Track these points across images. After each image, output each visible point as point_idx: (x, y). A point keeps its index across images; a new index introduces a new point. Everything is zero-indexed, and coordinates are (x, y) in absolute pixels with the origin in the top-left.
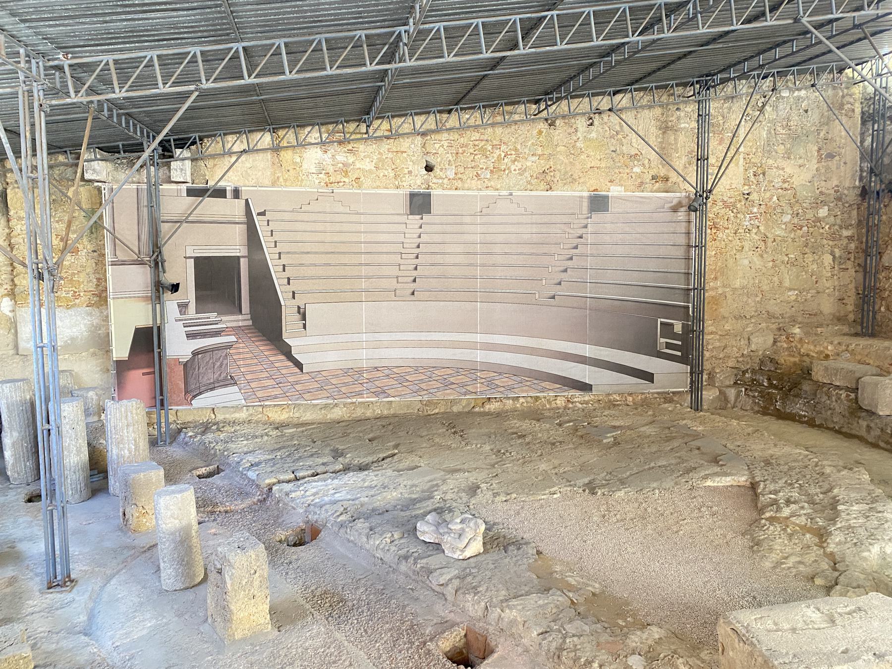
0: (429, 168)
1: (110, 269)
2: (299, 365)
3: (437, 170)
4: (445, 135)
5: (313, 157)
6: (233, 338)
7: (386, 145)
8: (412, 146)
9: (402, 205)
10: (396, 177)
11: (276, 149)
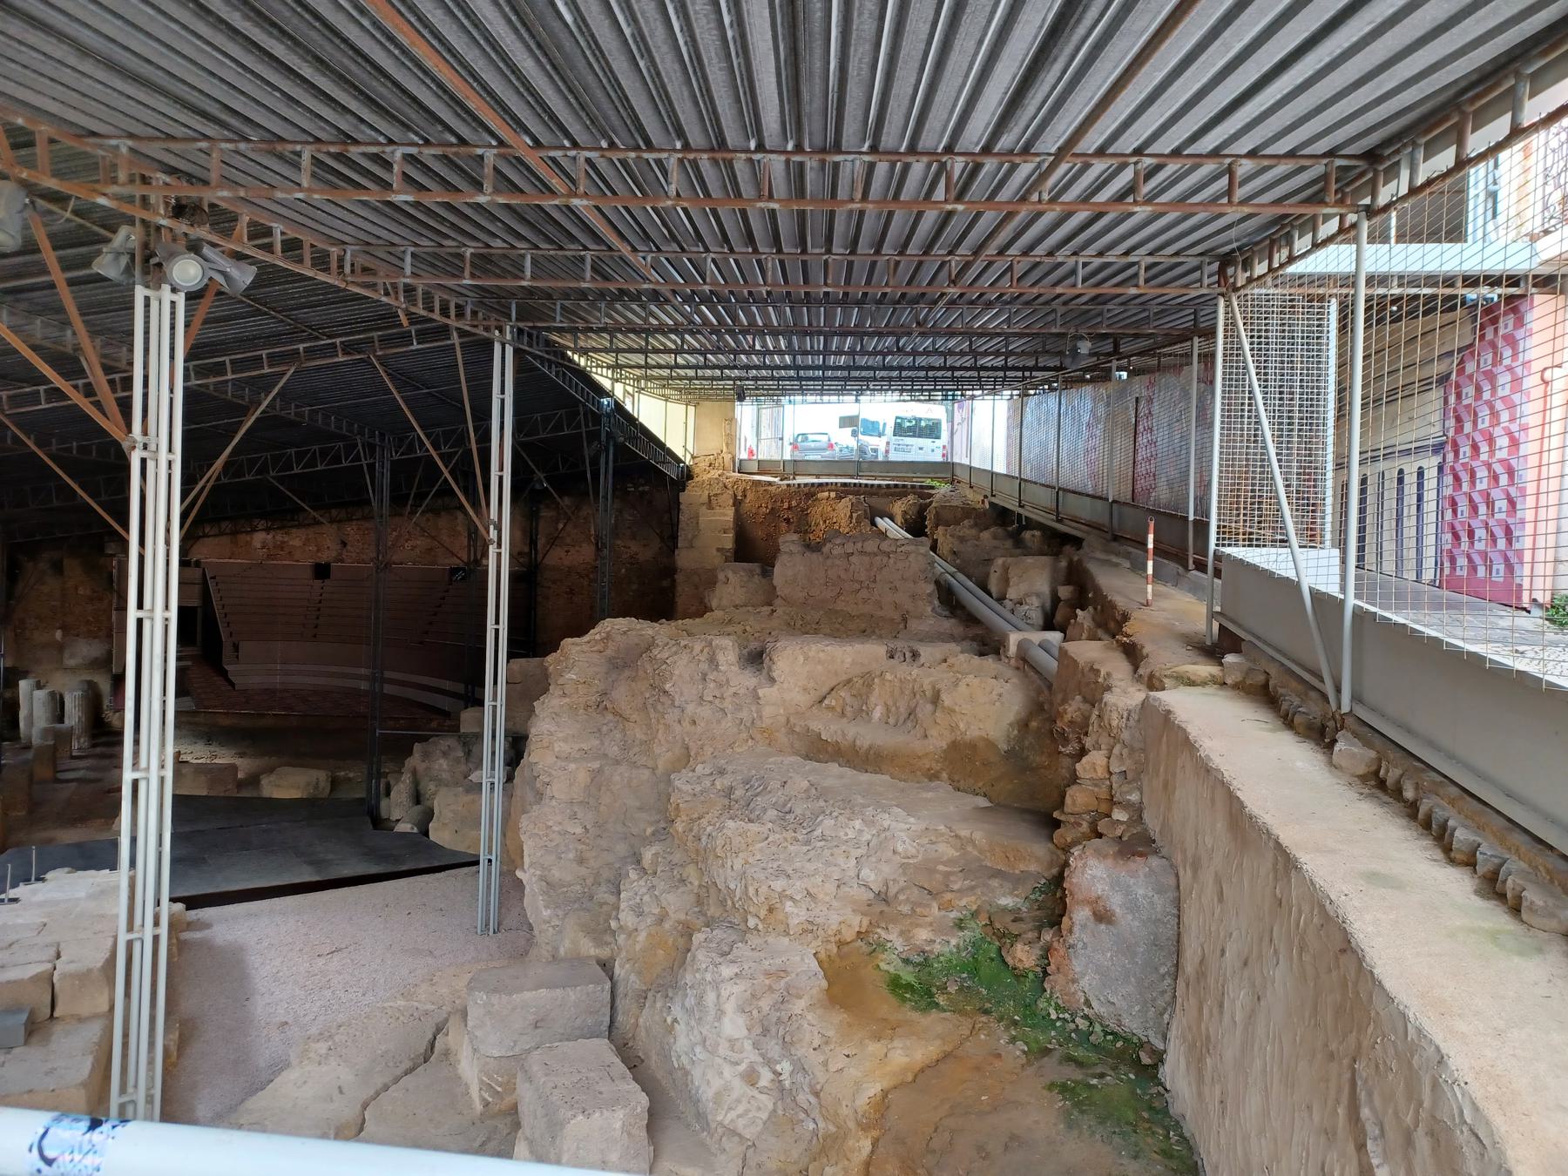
0: (344, 544)
1: (114, 613)
2: (232, 684)
3: (349, 547)
5: (259, 538)
6: (189, 663)
10: (318, 551)
11: (234, 533)
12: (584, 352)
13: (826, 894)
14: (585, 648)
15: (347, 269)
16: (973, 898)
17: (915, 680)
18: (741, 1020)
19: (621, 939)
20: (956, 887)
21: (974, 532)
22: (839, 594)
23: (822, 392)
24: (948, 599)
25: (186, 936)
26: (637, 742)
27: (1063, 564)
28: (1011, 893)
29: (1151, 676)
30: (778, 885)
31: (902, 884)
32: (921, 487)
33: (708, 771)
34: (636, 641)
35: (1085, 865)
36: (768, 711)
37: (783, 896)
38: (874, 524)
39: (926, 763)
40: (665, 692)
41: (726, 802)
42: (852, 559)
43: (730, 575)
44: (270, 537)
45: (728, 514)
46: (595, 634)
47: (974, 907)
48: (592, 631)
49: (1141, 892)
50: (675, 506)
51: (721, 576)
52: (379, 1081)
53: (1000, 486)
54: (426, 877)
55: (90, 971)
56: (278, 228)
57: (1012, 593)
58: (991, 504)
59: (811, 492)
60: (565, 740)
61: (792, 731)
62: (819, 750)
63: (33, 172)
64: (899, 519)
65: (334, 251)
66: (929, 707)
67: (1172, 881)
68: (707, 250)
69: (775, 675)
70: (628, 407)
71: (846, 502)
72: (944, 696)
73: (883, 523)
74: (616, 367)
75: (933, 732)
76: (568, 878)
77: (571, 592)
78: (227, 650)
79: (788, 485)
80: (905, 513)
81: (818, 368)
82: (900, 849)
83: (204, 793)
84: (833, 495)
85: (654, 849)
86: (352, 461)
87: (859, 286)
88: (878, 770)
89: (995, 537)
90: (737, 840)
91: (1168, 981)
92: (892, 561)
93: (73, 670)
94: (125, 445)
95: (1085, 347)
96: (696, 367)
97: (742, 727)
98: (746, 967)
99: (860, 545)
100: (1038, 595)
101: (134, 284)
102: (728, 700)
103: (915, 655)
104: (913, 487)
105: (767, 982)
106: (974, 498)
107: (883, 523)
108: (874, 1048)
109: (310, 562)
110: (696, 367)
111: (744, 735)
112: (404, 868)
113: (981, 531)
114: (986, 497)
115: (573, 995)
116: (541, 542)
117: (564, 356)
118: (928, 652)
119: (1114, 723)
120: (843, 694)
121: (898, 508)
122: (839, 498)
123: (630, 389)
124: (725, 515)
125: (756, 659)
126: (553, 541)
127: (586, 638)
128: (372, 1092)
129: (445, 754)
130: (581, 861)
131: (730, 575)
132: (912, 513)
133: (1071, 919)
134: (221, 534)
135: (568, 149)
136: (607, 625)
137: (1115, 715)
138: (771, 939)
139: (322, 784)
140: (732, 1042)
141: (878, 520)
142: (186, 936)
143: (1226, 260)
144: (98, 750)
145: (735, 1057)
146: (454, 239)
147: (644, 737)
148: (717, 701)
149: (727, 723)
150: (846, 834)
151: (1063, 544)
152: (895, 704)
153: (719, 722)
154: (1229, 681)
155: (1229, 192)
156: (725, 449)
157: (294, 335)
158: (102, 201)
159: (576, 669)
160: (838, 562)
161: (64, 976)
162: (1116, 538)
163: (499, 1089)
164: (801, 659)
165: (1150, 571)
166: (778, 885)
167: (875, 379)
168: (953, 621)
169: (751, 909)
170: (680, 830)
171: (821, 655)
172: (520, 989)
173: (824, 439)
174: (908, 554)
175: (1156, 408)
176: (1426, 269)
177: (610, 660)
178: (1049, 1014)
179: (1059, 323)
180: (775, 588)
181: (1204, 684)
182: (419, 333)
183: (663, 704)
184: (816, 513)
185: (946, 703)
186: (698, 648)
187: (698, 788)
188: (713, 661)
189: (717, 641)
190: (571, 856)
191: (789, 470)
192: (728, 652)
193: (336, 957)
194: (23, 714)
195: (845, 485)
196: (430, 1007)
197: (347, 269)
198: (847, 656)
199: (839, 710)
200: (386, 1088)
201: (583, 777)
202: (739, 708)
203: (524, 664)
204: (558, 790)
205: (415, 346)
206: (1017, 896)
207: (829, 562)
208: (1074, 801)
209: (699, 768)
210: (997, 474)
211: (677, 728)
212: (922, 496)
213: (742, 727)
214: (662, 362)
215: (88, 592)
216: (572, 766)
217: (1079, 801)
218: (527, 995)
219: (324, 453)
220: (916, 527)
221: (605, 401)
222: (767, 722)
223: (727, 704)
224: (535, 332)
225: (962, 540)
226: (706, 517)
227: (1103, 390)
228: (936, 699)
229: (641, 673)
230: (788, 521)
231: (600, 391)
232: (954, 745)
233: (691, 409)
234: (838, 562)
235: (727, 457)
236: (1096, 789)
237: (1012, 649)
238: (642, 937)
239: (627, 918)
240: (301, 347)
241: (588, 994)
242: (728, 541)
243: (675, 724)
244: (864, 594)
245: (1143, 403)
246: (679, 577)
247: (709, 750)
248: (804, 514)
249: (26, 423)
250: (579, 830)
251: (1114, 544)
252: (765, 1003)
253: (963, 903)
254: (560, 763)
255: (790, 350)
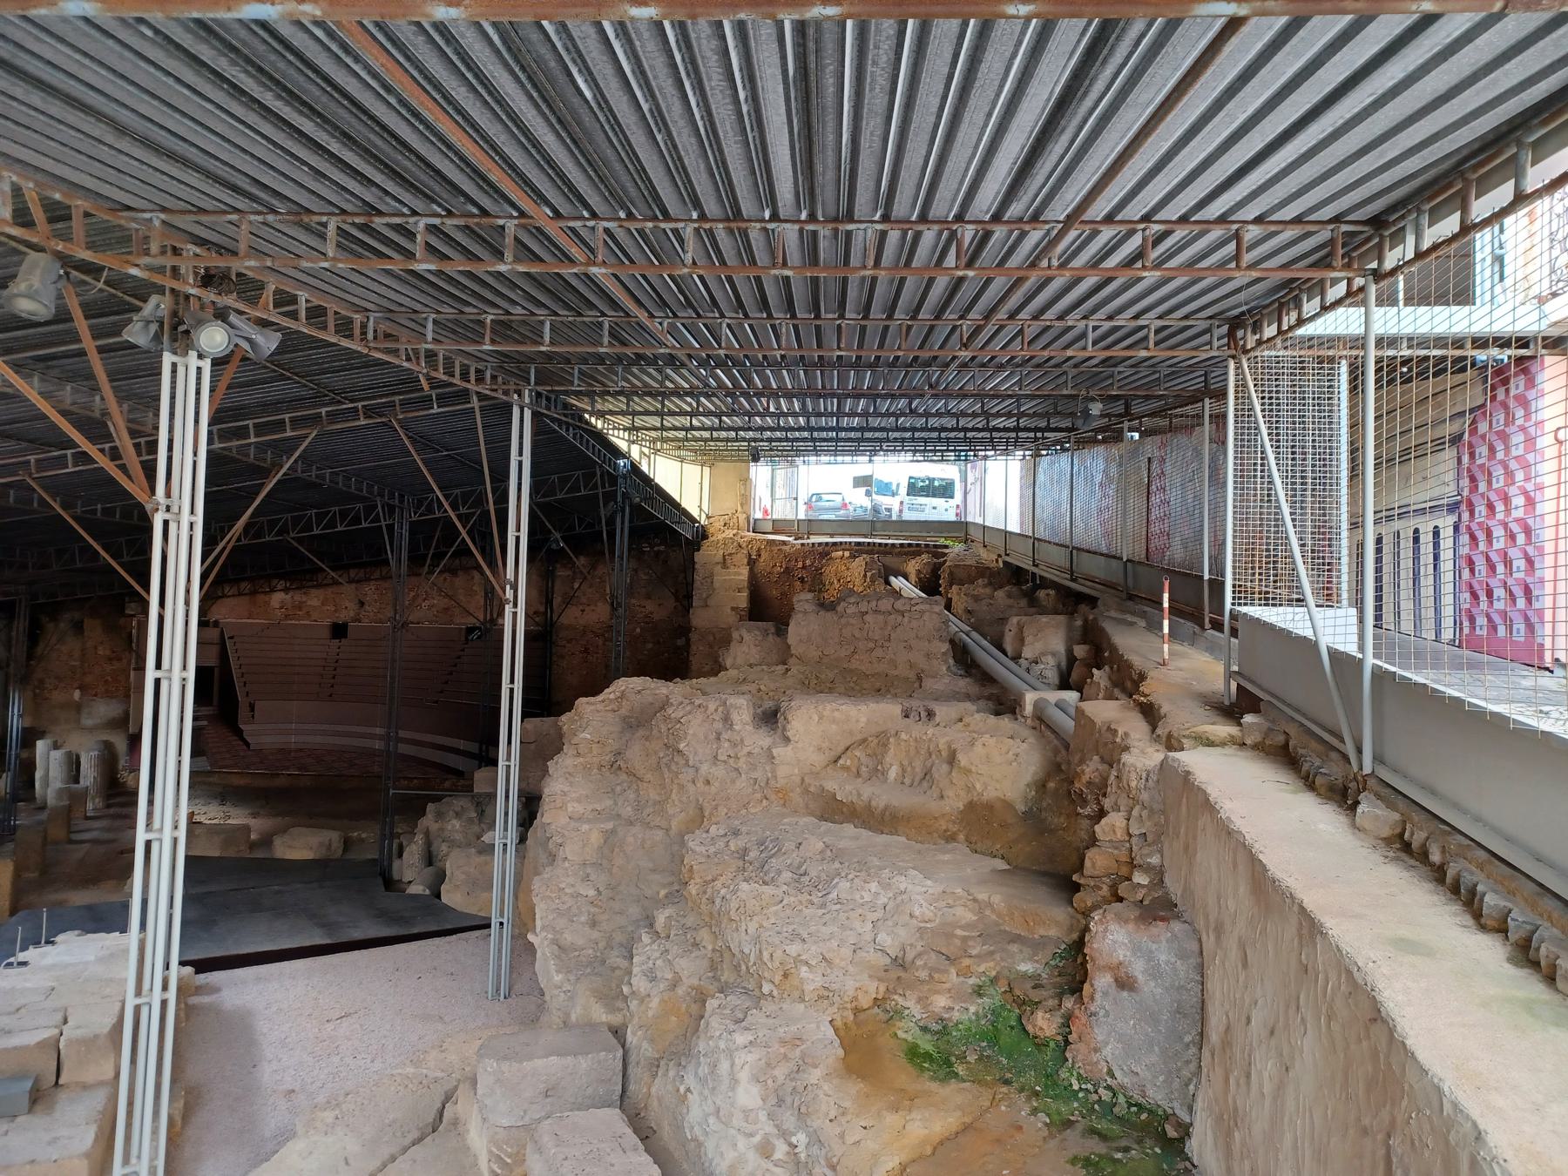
0: (362, 604)
1: (132, 673)
2: (247, 744)
4: (372, 583)
5: (277, 598)
6: (205, 723)
7: (330, 590)
8: (349, 589)
9: (326, 633)
10: (336, 611)
11: (254, 593)
12: (601, 414)
13: (842, 959)
14: (600, 707)
15: (370, 336)
16: (992, 964)
17: (930, 740)
18: (755, 1090)
19: (633, 1004)
20: (974, 952)
21: (988, 591)
22: (854, 652)
23: (835, 453)
24: (963, 658)
25: (194, 1000)
26: (650, 802)
27: (1079, 623)
28: (1031, 959)
29: (1169, 736)
30: (793, 949)
31: (919, 948)
32: (935, 546)
33: (722, 832)
34: (650, 699)
35: (1106, 931)
36: (782, 771)
37: (798, 960)
38: (888, 583)
39: (943, 825)
40: (679, 751)
41: (741, 863)
42: (868, 618)
43: (747, 637)
44: (288, 597)
45: (744, 573)
46: (610, 693)
47: (994, 973)
48: (607, 691)
49: (1163, 958)
50: (690, 565)
51: (735, 635)
52: (385, 1152)
53: (1012, 546)
54: (437, 941)
55: (96, 1037)
56: (303, 296)
57: (1028, 652)
58: (1005, 563)
59: (825, 552)
60: (579, 801)
61: (806, 791)
62: (833, 811)
63: (69, 245)
64: (913, 577)
65: (358, 318)
66: (945, 767)
67: (1195, 946)
68: (722, 316)
69: (789, 734)
70: (644, 468)
71: (859, 564)
72: (960, 756)
73: (897, 582)
74: (632, 429)
75: (950, 793)
76: (581, 942)
77: (586, 651)
78: (243, 711)
79: (803, 545)
80: (919, 572)
81: (832, 429)
82: (917, 913)
83: (217, 854)
84: (847, 554)
85: (668, 912)
86: (372, 522)
87: (871, 349)
88: (894, 832)
89: (1009, 596)
90: (751, 903)
91: (1193, 1050)
92: (906, 619)
93: (91, 730)
94: (148, 507)
95: (1096, 409)
96: (712, 429)
97: (757, 787)
98: (760, 1035)
99: (874, 603)
100: (1054, 655)
101: (162, 350)
102: (742, 760)
103: (930, 714)
104: (927, 546)
105: (782, 1050)
106: (987, 557)
107: (897, 582)
108: (892, 1119)
109: (327, 622)
110: (712, 429)
111: (758, 796)
112: (415, 931)
113: (996, 590)
114: (999, 556)
115: (584, 1063)
116: (557, 601)
117: (581, 419)
118: (943, 711)
119: (1133, 784)
120: (858, 754)
121: (912, 566)
122: (853, 557)
123: (646, 450)
124: (739, 574)
125: (770, 718)
126: (569, 601)
127: (600, 697)
128: (378, 1163)
129: (458, 815)
130: (593, 924)
131: (747, 637)
132: (926, 571)
133: (1092, 985)
134: (240, 594)
135: (588, 219)
136: (622, 684)
137: (1133, 776)
138: (785, 1006)
139: (335, 845)
140: (746, 1112)
141: (892, 579)
142: (194, 1000)
143: (1236, 323)
144: (112, 811)
145: (750, 1128)
146: (475, 307)
147: (658, 798)
148: (731, 761)
149: (742, 783)
150: (862, 897)
151: (1077, 603)
152: (910, 763)
153: (733, 781)
154: (1248, 742)
155: (1237, 257)
156: (739, 509)
157: (317, 399)
158: (134, 271)
159: (590, 729)
160: (852, 621)
161: (70, 1042)
162: (1131, 597)
163: (509, 1161)
164: (816, 718)
165: (1166, 630)
166: (793, 949)
167: (888, 440)
168: (968, 680)
169: (766, 975)
170: (694, 892)
171: (836, 714)
172: (530, 1058)
173: (838, 499)
174: (922, 612)
175: (1168, 468)
176: (1435, 331)
177: (624, 719)
178: (1071, 1085)
179: (1070, 385)
180: (789, 647)
181: (1223, 744)
182: (439, 397)
183: (677, 764)
184: (830, 571)
185: (962, 764)
186: (712, 707)
187: (712, 850)
188: (726, 719)
189: (732, 700)
190: (583, 919)
191: (804, 529)
192: (742, 711)
193: (345, 1023)
194: (38, 775)
195: (858, 544)
196: (440, 1074)
197: (370, 336)
198: (862, 715)
199: (854, 770)
200: (393, 1159)
201: (595, 838)
202: (753, 767)
203: (538, 724)
204: (571, 851)
205: (436, 410)
206: (1037, 961)
207: (843, 621)
208: (1094, 865)
209: (713, 829)
210: (1011, 533)
211: (691, 788)
212: (936, 555)
213: (757, 787)
214: (677, 424)
215: (108, 653)
216: (585, 827)
217: (1099, 863)
218: (539, 1063)
219: (343, 514)
220: (930, 585)
221: (621, 462)
222: (781, 782)
223: (742, 764)
224: (553, 397)
225: (977, 599)
226: (721, 576)
227: (1115, 450)
228: (952, 759)
229: (655, 732)
230: (802, 580)
231: (616, 452)
232: (971, 806)
233: (707, 470)
234: (852, 621)
235: (742, 517)
236: (1116, 852)
237: (1029, 709)
238: (655, 1003)
239: (640, 983)
240: (324, 410)
241: (599, 1062)
242: (742, 600)
243: (690, 784)
244: (879, 652)
245: (1154, 465)
246: (694, 637)
247: (723, 811)
248: (818, 575)
249: (53, 486)
250: (592, 893)
251: (1130, 603)
252: (780, 1072)
253: (981, 969)
254: (573, 824)
255: (804, 412)
